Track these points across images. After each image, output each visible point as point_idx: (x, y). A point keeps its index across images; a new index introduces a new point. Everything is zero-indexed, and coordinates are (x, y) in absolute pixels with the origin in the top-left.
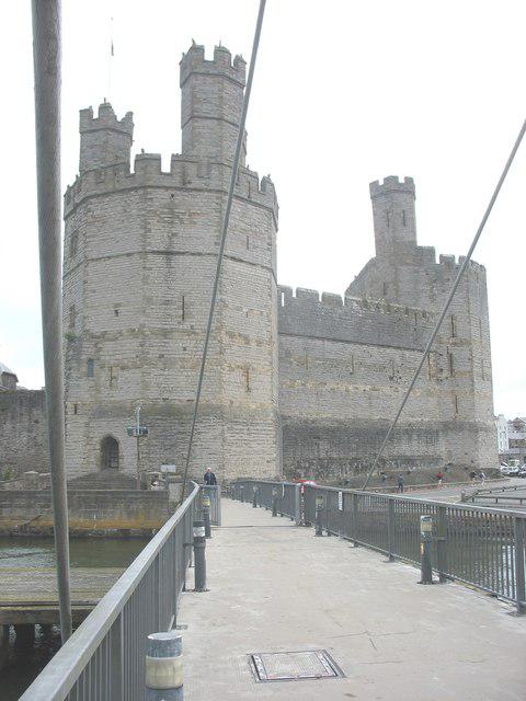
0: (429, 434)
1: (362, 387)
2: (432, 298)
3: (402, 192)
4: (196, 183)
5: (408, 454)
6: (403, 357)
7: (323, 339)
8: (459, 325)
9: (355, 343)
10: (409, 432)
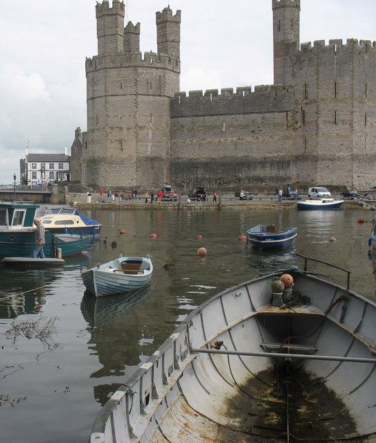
0: (282, 163)
1: (230, 139)
2: (294, 75)
3: (279, 8)
4: (99, 67)
5: (262, 175)
6: (263, 118)
7: (204, 116)
8: (310, 90)
9: (226, 114)
10: (263, 163)
